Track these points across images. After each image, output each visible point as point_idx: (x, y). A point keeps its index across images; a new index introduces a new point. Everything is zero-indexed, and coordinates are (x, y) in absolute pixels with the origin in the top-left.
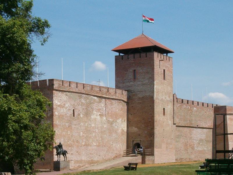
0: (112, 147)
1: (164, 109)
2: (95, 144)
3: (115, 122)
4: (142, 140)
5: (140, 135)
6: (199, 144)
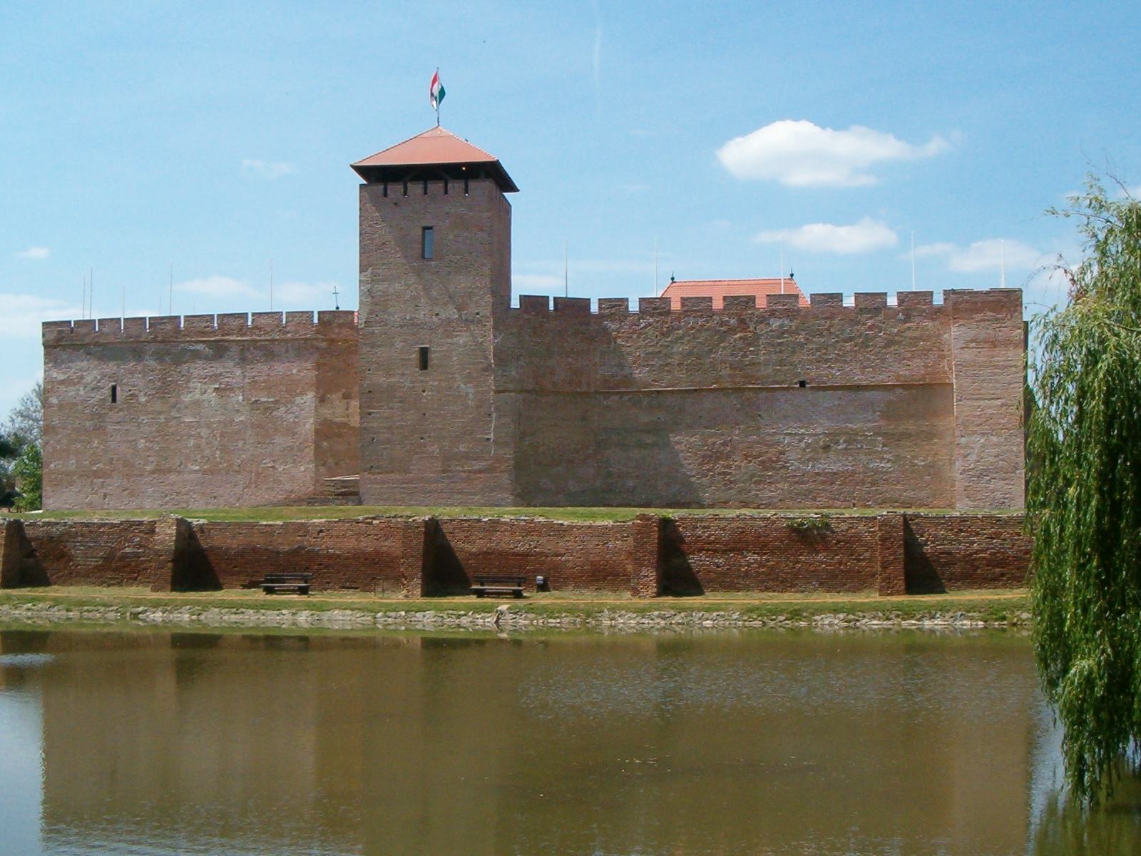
2: (197, 468)
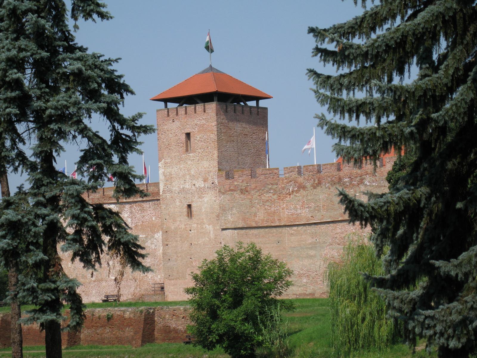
1: (189, 206)
3: (150, 239)
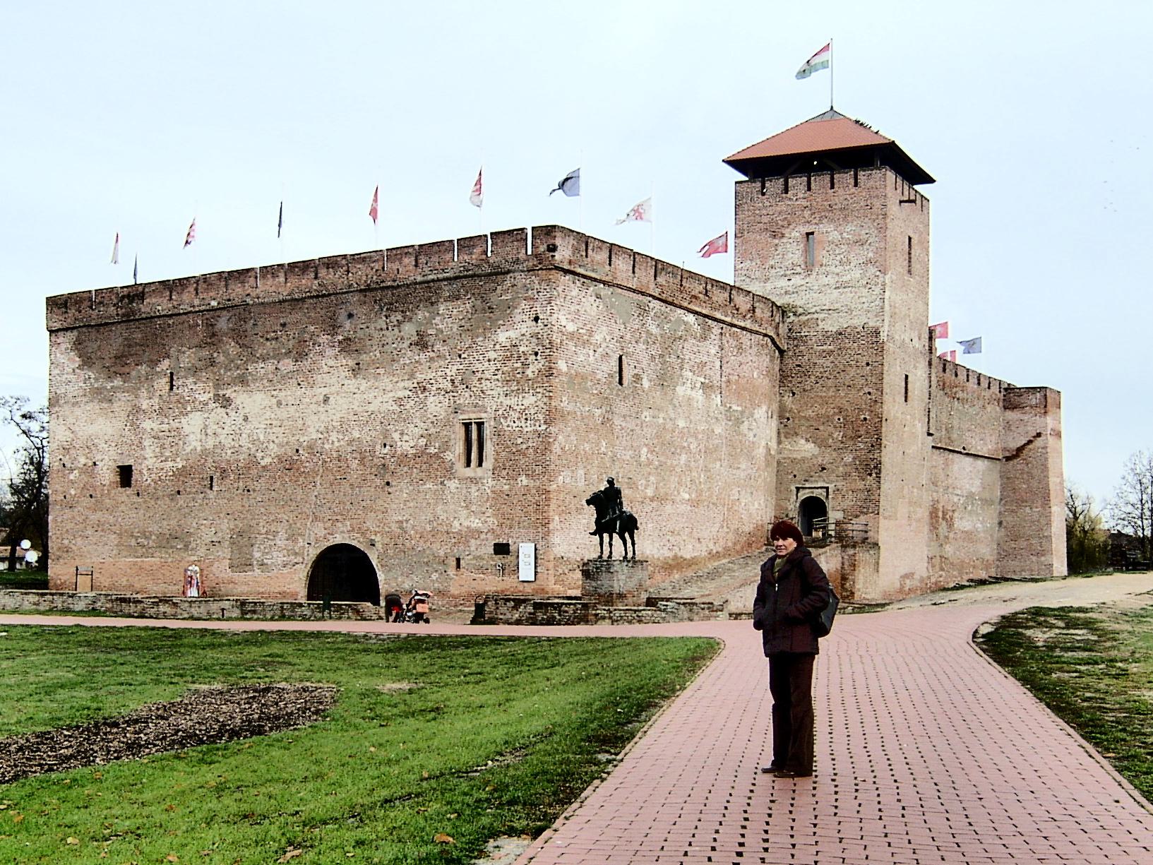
0: (736, 508)
1: (907, 377)
2: (687, 496)
4: (831, 486)
5: (824, 469)
6: (965, 508)
